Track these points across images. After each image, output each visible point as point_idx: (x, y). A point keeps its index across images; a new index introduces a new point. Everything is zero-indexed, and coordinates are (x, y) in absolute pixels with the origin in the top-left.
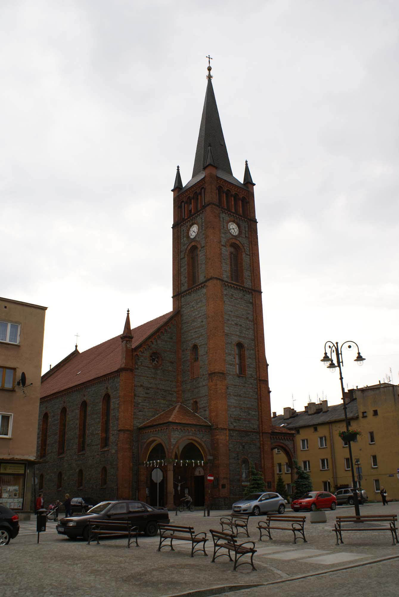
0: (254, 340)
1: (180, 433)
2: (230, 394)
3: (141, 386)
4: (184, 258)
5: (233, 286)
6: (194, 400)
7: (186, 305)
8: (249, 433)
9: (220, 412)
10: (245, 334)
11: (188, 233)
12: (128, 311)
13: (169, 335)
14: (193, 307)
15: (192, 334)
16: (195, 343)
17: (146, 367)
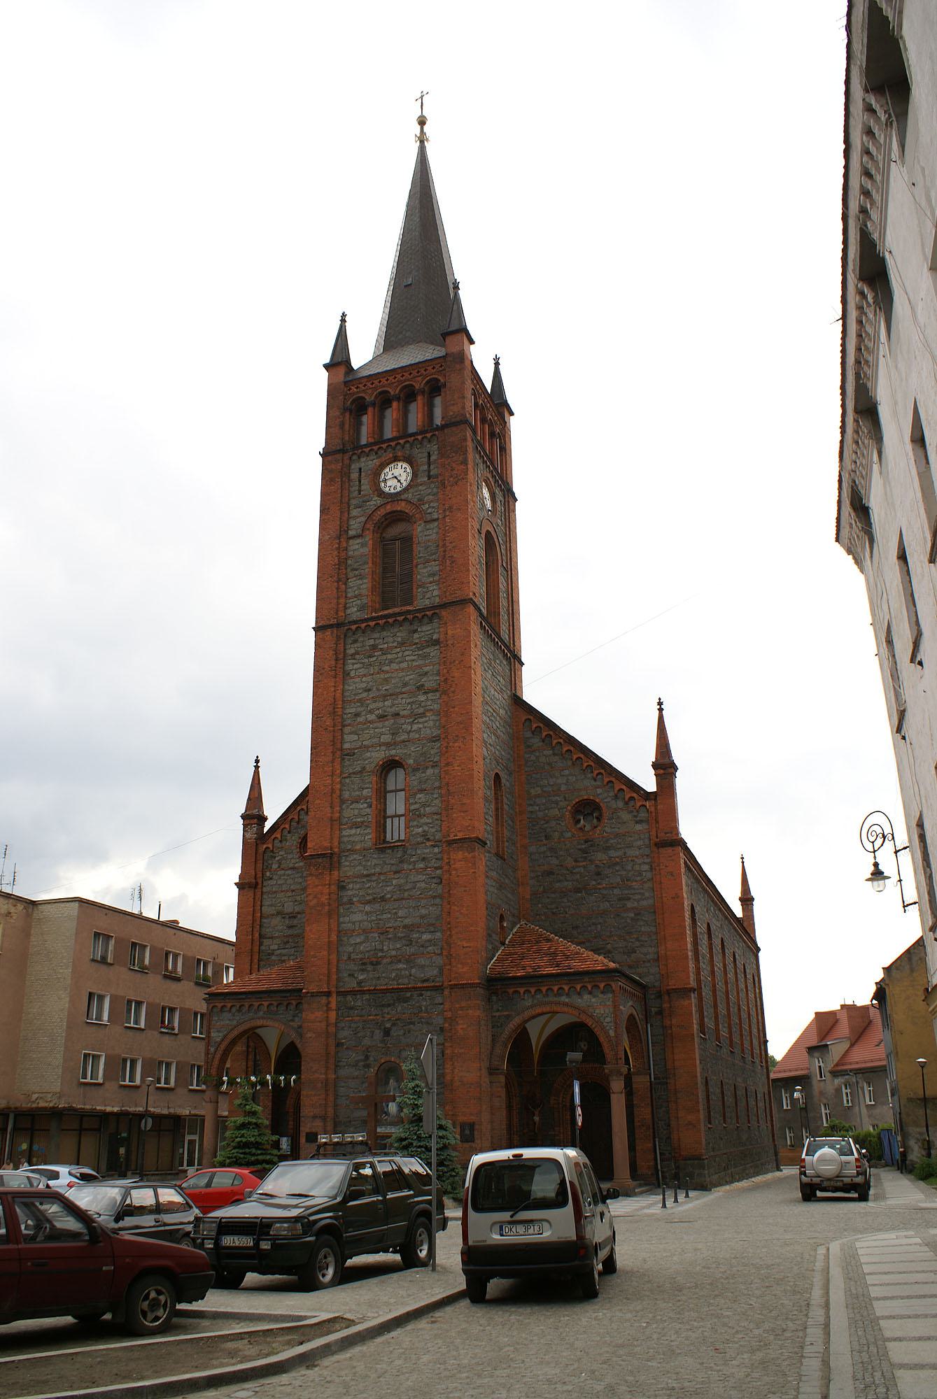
0: (435, 739)
2: (351, 902)
3: (278, 913)
8: (408, 994)
12: (257, 761)
17: (291, 869)
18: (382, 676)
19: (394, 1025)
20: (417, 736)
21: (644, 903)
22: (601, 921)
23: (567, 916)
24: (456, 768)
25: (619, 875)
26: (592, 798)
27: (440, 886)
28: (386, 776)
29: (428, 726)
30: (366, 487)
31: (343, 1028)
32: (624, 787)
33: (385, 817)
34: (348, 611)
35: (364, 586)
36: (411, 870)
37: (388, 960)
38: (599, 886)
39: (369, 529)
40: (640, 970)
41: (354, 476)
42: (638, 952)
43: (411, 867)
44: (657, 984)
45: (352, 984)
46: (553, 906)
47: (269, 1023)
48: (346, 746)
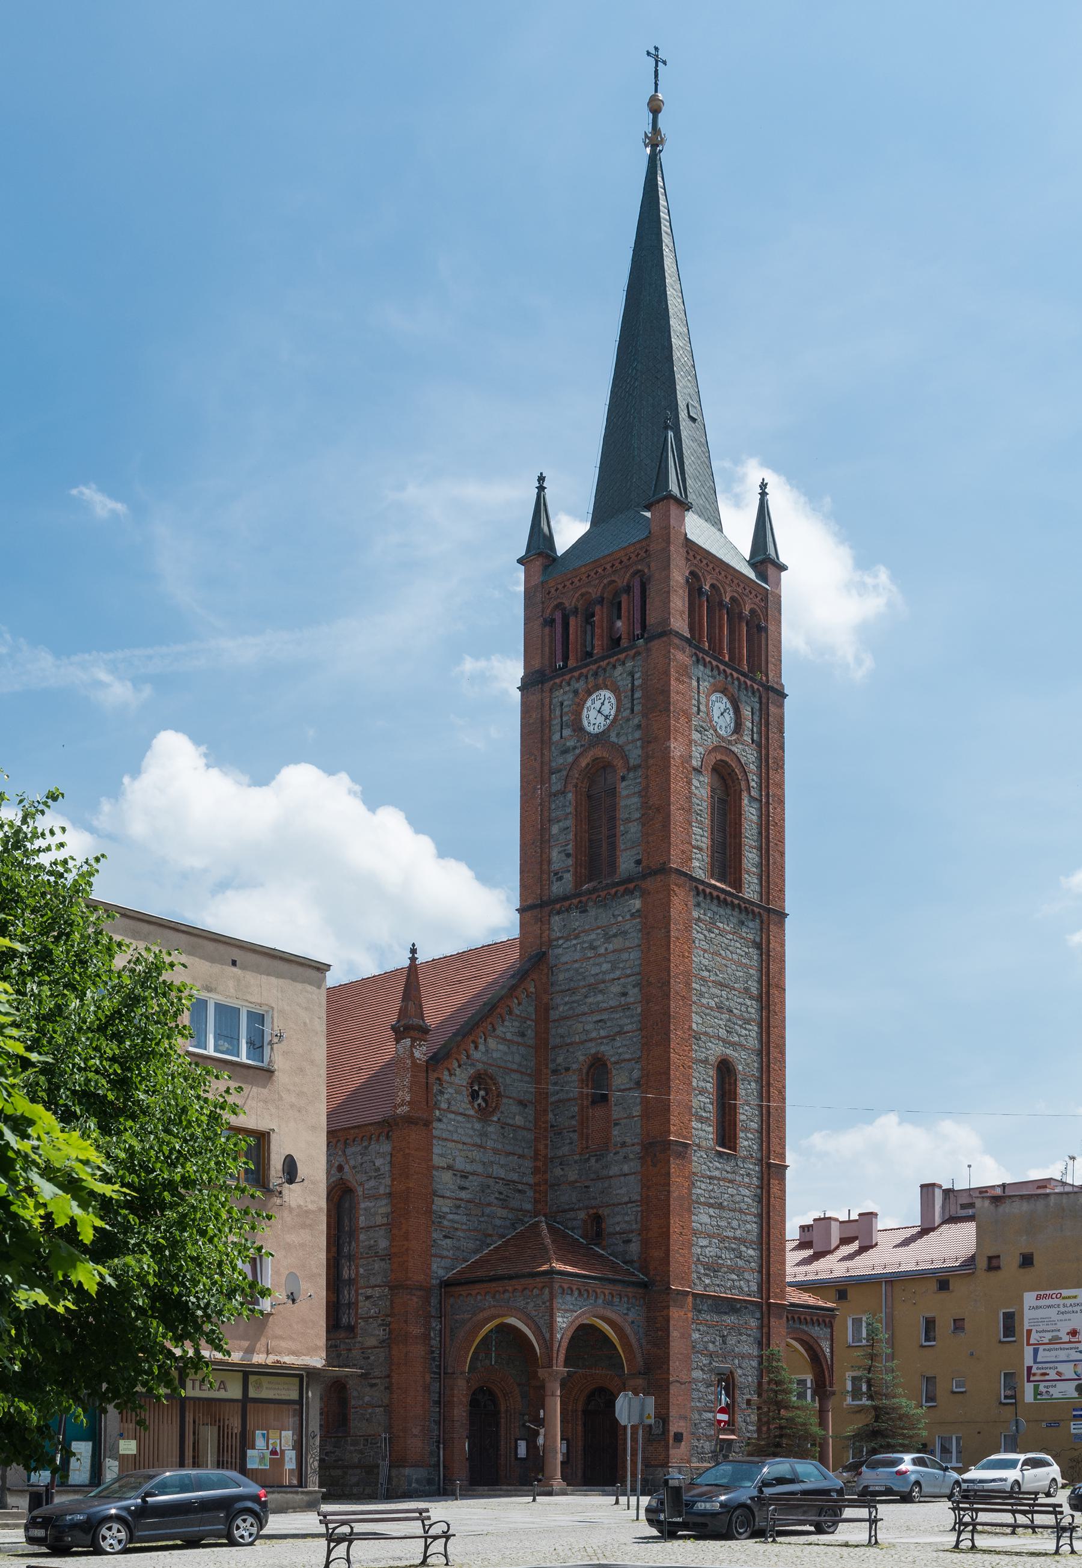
3: (449, 1167)
4: (563, 792)
5: (715, 893)
6: (591, 1211)
7: (567, 940)
10: (740, 1036)
11: (578, 714)
13: (516, 1024)
14: (593, 948)
15: (587, 1027)
16: (598, 1053)
17: (461, 1114)
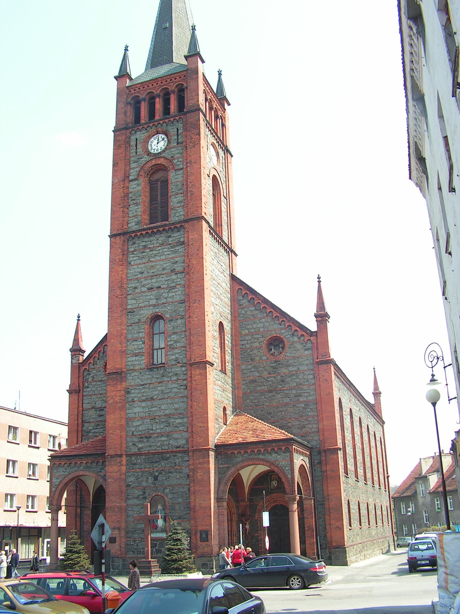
0: (182, 302)
1: (66, 469)
2: (133, 401)
3: (93, 408)
8: (168, 455)
9: (111, 432)
18: (150, 264)
19: (160, 473)
20: (171, 300)
21: (310, 398)
22: (285, 409)
23: (264, 406)
24: (195, 319)
25: (295, 382)
26: (278, 335)
27: (186, 391)
28: (153, 324)
29: (178, 294)
30: (140, 150)
31: (130, 476)
32: (298, 329)
33: (153, 350)
34: (130, 225)
35: (140, 210)
36: (168, 381)
37: (156, 435)
38: (283, 389)
39: (141, 175)
40: (308, 438)
41: (133, 143)
42: (307, 427)
43: (169, 379)
44: (318, 446)
45: (134, 450)
46: (256, 401)
47: (87, 473)
48: (129, 307)
